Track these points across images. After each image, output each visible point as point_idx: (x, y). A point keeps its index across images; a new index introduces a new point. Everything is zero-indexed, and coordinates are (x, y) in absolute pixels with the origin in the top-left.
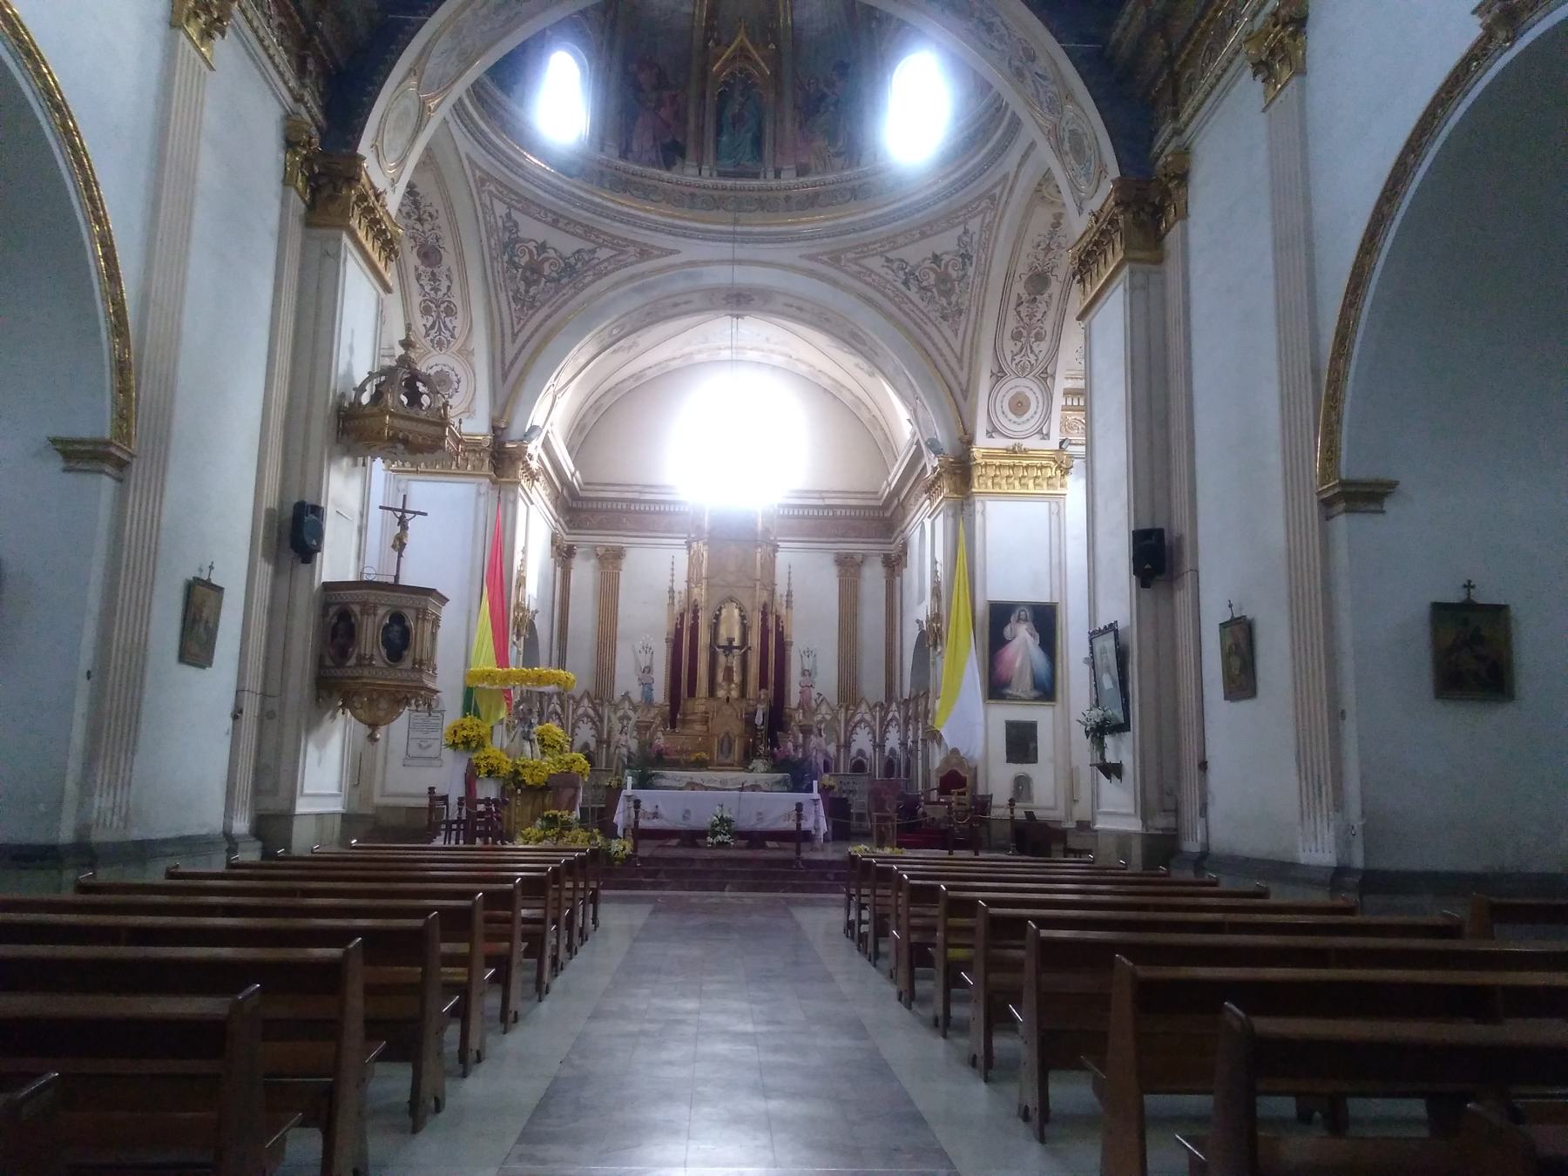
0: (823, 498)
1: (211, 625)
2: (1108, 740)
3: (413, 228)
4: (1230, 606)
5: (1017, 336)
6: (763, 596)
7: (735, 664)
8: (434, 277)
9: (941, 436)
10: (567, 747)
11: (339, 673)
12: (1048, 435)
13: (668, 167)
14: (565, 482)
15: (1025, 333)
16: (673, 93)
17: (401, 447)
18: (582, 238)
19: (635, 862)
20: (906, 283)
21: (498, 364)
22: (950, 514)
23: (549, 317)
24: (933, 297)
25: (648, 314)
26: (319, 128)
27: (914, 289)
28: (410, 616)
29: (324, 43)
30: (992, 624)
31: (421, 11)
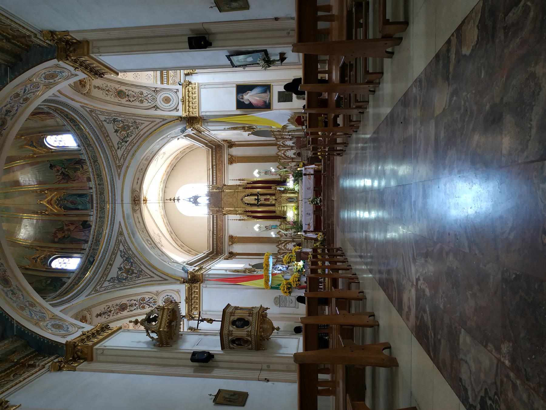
1: (233, 393)
2: (272, 58)
3: (114, 313)
4: (212, 7)
5: (142, 102)
6: (240, 189)
7: (262, 198)
8: (131, 306)
9: (180, 128)
10: (291, 254)
11: (253, 343)
12: (177, 90)
13: (90, 226)
14: (207, 256)
15: (140, 99)
16: (65, 225)
17: (173, 323)
18: (116, 256)
19: (325, 231)
20: (126, 142)
22: (207, 124)
25: (143, 231)
26: (56, 358)
27: (128, 139)
28: (232, 318)
29: (23, 358)
31: (13, 322)
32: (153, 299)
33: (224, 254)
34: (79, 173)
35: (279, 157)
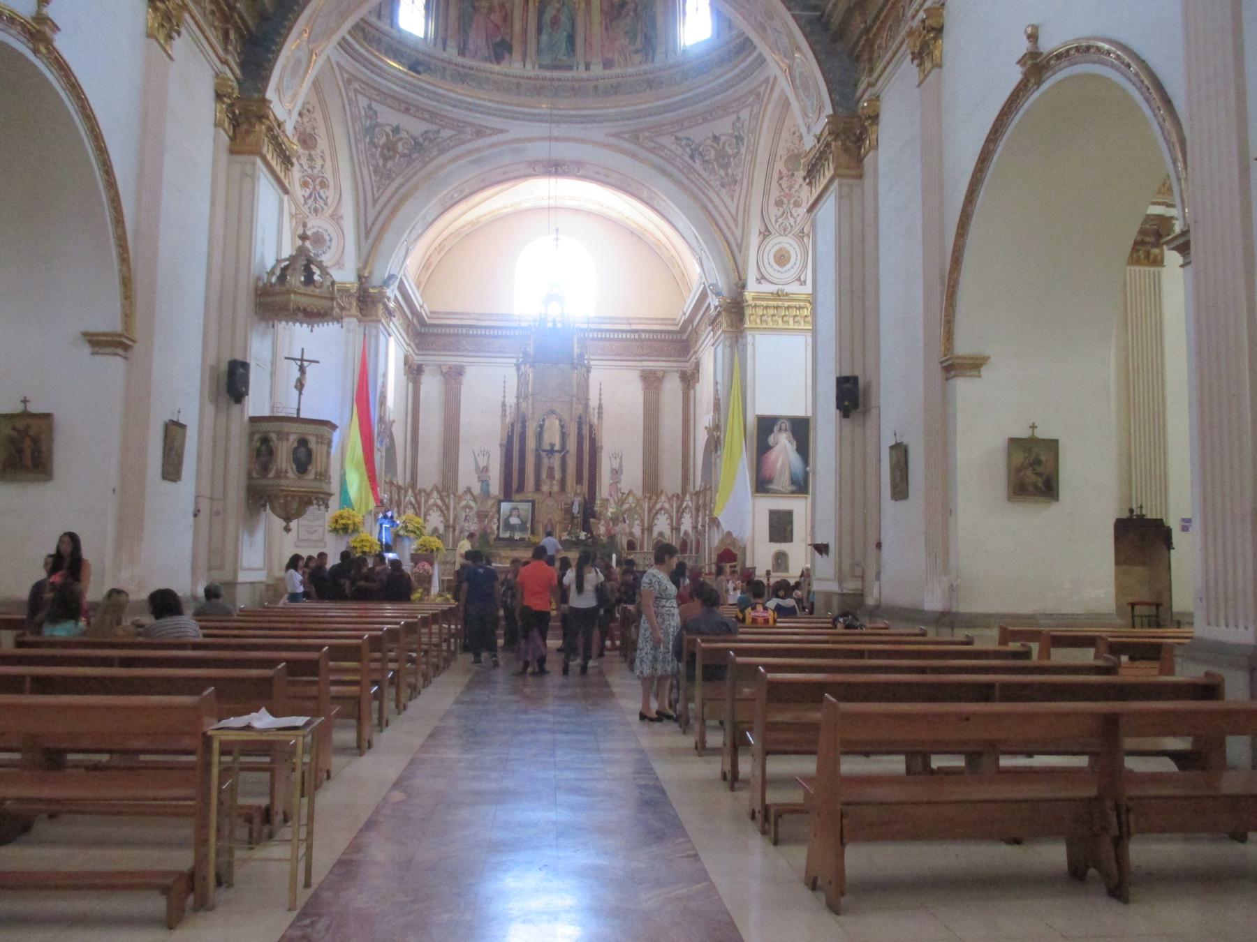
0: (630, 324)
4: (895, 434)
5: (779, 203)
6: (578, 410)
7: (556, 461)
8: (311, 158)
9: (722, 284)
11: (262, 482)
12: (805, 282)
15: (785, 201)
17: (301, 315)
18: (428, 121)
20: (692, 157)
21: (362, 226)
22: (727, 343)
23: (402, 185)
24: (713, 169)
27: (698, 162)
29: (241, 18)
30: (758, 436)
32: (324, 206)
33: (416, 351)
34: (623, 41)
35: (654, 497)
